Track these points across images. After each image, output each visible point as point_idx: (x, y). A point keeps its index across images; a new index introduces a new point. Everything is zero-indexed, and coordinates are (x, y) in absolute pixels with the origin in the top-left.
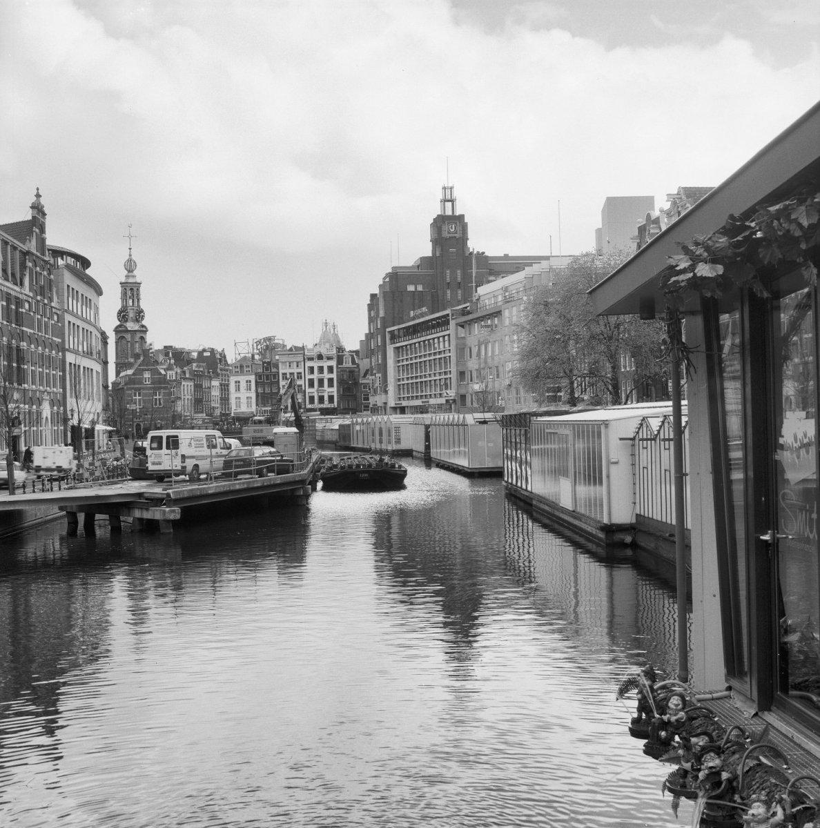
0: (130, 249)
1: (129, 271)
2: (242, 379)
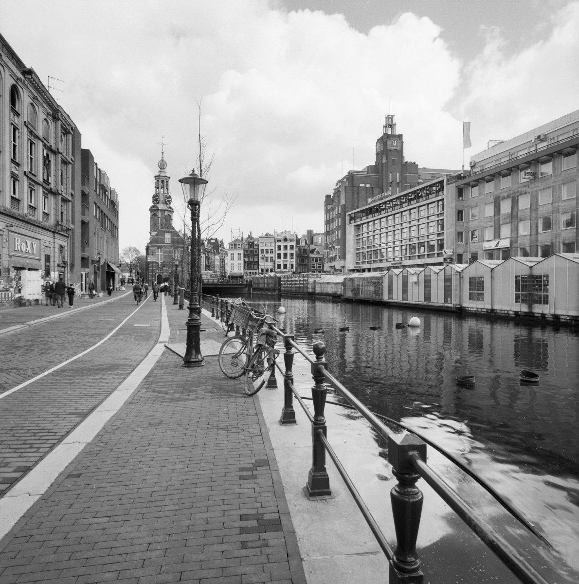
0: (163, 153)
1: (161, 169)
2: (236, 252)
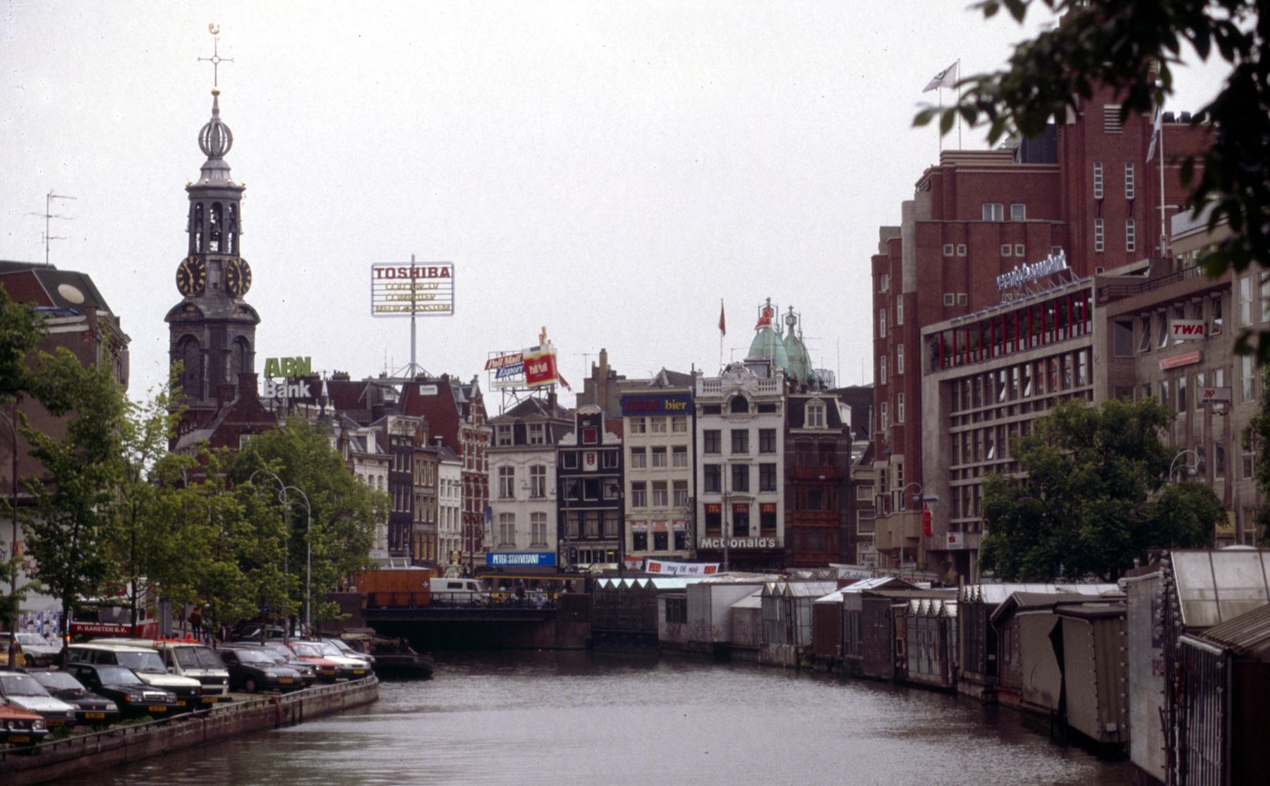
0: (216, 93)
2: (522, 464)
